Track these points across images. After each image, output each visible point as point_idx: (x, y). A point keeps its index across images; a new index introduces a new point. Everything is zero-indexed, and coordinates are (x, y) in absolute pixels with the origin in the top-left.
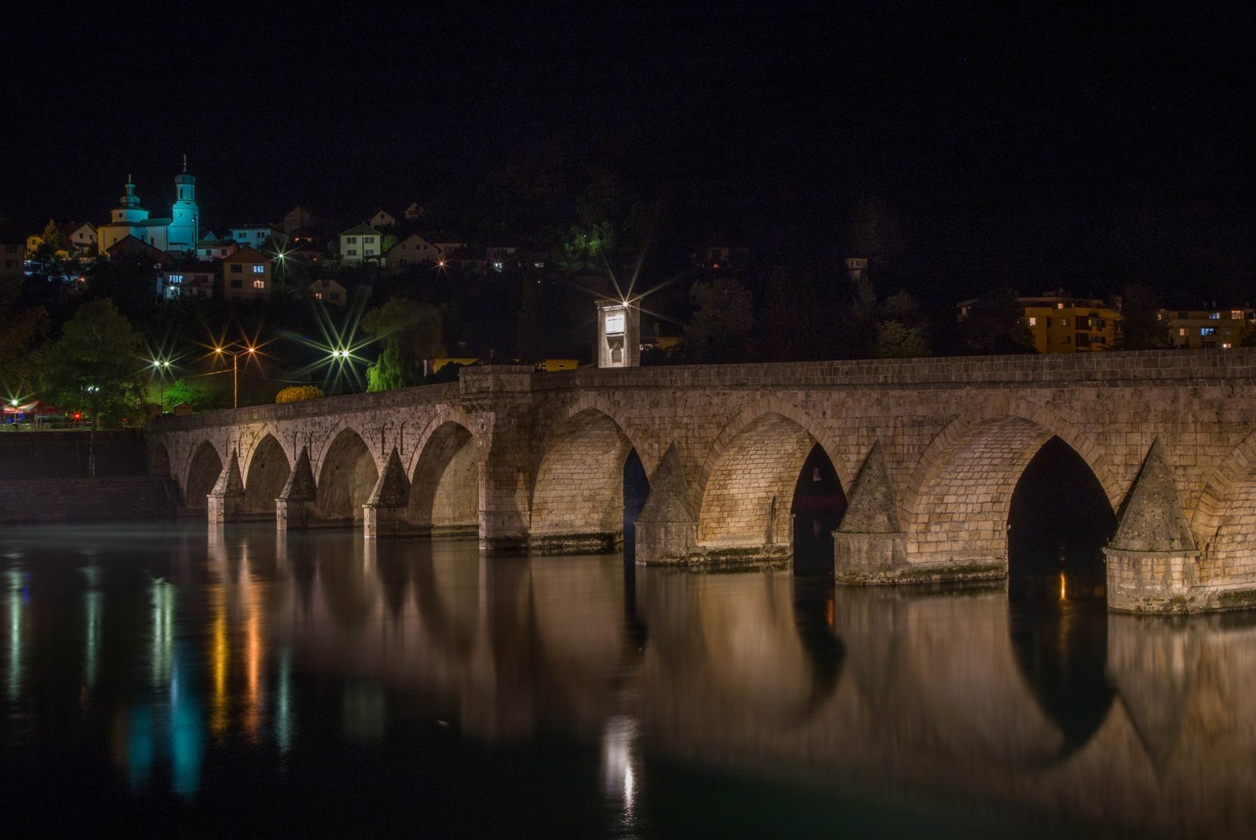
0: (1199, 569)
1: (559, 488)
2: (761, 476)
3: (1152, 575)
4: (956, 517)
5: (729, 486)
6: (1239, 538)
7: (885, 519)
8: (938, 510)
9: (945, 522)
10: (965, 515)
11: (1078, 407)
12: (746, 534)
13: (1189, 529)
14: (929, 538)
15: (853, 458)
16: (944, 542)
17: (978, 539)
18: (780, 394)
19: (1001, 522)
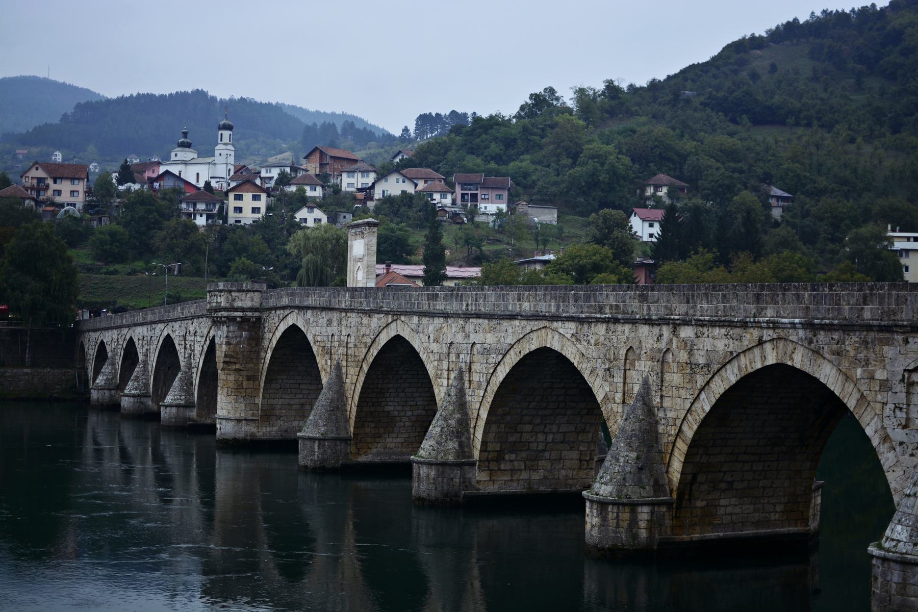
0: (671, 518)
1: (287, 396)
2: (417, 395)
3: (618, 524)
4: (534, 446)
5: (383, 404)
6: (723, 486)
7: (456, 445)
8: (511, 439)
9: (521, 451)
10: (544, 444)
11: (592, 341)
12: (404, 450)
13: (665, 475)
14: (502, 467)
15: (445, 382)
16: (520, 470)
17: (563, 469)
18: (403, 318)
19: (589, 452)
